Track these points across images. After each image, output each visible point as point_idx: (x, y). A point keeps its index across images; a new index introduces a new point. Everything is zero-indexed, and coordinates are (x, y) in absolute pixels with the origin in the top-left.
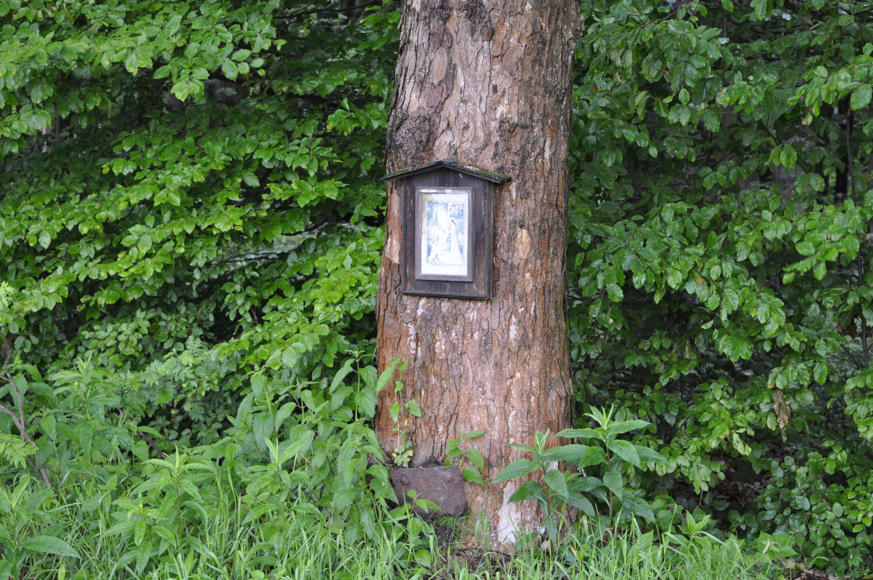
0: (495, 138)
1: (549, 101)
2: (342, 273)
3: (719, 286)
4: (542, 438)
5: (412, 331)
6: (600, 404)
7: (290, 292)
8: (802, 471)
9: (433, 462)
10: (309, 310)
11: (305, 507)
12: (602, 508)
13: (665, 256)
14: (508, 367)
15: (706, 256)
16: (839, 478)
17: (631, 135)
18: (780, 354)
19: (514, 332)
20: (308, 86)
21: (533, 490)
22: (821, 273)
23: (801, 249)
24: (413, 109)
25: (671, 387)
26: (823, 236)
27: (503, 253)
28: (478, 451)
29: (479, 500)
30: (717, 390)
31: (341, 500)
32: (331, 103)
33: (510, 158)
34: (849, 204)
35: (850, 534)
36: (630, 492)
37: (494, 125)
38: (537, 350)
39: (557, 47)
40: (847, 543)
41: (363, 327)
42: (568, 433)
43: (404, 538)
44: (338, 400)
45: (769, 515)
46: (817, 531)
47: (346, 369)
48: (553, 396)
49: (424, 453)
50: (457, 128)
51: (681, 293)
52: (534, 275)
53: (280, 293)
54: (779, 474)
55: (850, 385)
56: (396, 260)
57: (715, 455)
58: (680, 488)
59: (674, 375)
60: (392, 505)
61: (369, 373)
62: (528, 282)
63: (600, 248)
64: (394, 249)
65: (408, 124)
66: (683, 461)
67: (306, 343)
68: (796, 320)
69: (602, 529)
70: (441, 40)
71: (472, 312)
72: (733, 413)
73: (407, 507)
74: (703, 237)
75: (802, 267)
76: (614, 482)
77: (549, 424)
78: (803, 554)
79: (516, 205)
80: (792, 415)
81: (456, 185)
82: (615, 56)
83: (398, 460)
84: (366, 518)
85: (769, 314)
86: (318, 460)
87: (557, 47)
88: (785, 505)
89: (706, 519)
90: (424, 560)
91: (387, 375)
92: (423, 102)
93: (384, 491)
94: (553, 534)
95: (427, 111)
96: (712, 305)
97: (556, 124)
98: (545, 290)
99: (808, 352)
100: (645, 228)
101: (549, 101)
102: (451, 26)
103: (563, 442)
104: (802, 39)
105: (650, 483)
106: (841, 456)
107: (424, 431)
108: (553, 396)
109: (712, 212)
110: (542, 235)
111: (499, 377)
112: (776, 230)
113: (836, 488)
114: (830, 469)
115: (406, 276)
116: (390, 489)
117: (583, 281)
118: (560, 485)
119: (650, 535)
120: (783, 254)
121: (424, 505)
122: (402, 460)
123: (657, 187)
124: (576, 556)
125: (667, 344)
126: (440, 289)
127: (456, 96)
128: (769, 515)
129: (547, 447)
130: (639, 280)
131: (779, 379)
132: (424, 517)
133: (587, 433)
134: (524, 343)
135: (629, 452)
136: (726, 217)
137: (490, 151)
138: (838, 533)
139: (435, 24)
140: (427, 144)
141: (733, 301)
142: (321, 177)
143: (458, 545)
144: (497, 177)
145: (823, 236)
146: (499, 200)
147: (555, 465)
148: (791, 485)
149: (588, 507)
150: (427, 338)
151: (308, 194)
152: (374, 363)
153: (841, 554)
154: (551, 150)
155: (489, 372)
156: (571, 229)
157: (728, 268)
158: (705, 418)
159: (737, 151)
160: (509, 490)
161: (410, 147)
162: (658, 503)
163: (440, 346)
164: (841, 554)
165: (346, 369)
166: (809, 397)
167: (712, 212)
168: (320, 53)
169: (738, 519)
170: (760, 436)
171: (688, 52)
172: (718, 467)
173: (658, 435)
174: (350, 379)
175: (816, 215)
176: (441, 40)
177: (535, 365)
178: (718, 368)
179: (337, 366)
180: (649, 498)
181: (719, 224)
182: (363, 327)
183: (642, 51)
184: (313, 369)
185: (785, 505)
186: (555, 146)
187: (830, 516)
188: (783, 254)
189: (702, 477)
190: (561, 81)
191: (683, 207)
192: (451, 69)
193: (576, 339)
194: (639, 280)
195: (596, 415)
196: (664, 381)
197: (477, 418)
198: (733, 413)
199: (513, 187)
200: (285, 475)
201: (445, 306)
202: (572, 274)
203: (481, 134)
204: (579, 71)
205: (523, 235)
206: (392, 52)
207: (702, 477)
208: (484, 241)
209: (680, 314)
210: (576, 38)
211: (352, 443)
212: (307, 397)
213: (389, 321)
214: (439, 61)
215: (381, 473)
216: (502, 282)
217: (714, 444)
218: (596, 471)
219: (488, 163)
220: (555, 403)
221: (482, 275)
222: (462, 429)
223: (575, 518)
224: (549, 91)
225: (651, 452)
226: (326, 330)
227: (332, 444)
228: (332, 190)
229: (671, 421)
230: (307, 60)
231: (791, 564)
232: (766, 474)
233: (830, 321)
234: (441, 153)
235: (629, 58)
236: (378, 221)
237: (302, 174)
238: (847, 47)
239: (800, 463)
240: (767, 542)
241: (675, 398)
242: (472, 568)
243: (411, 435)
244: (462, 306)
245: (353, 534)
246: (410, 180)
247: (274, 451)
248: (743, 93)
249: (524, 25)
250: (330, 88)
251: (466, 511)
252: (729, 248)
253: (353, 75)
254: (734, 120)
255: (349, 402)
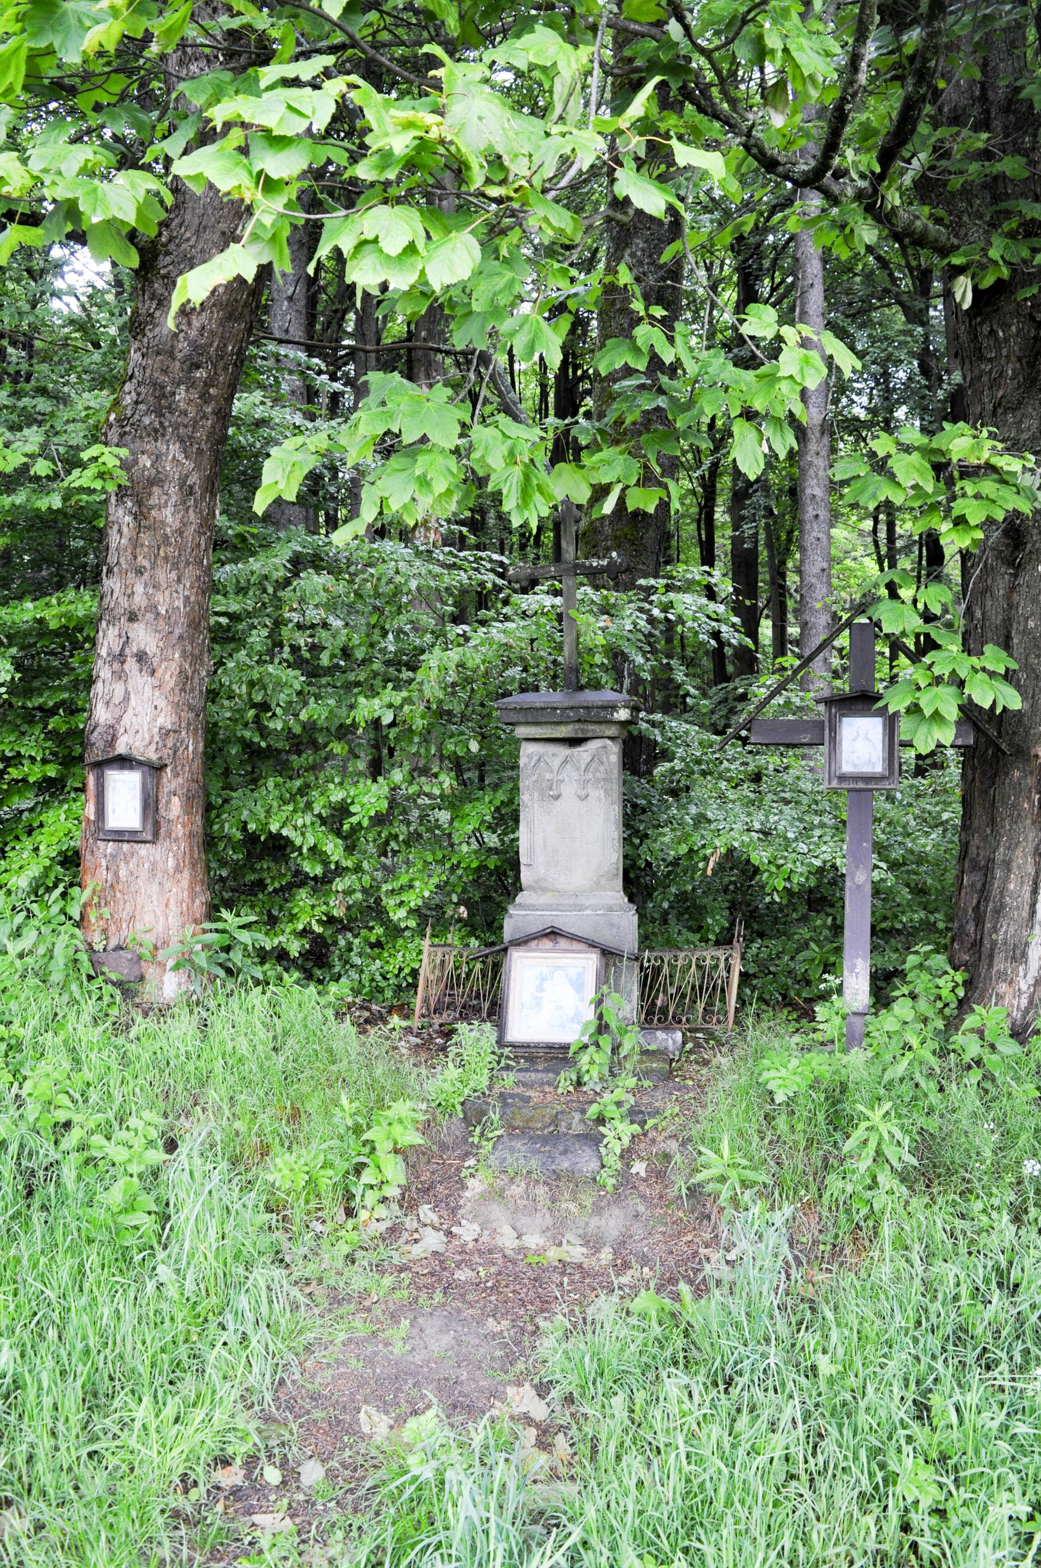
0: (157, 738)
1: (191, 715)
2: (57, 827)
3: (301, 830)
4: (190, 929)
5: (104, 863)
6: (229, 905)
7: (24, 838)
8: (357, 941)
9: (119, 948)
10: (36, 849)
11: (32, 981)
12: (229, 972)
13: (268, 812)
14: (168, 885)
15: (295, 811)
16: (378, 945)
17: (247, 734)
18: (340, 871)
19: (171, 863)
20: (38, 701)
21: (185, 963)
22: (365, 823)
23: (353, 809)
24: (102, 721)
25: (276, 891)
26: (365, 800)
27: (162, 812)
28: (149, 940)
29: (151, 972)
30: (303, 893)
31: (57, 977)
32: (52, 712)
33: (166, 751)
34: (380, 779)
35: (385, 978)
36: (249, 961)
37: (156, 730)
38: (186, 874)
39: (196, 680)
40: (383, 984)
41: (71, 860)
42: (208, 925)
43: (100, 999)
44: (55, 909)
45: (337, 969)
46: (366, 978)
47: (61, 889)
48: (198, 902)
49: (113, 943)
50: (131, 732)
51: (279, 836)
52: (184, 826)
53: (17, 838)
54: (342, 943)
55: (385, 887)
56: (92, 817)
57: (305, 932)
58: (281, 955)
59: (277, 885)
60: (90, 978)
61: (75, 891)
62: (179, 831)
63: (227, 806)
64: (90, 811)
65: (99, 730)
66: (282, 939)
67: (34, 870)
68: (350, 849)
69: (230, 985)
70: (120, 675)
71: (143, 850)
72: (313, 907)
73: (101, 978)
74: (293, 798)
75: (354, 820)
76: (236, 957)
77: (196, 922)
78: (356, 992)
79: (171, 782)
80: (349, 908)
81: (131, 768)
82: (235, 687)
83: (96, 948)
84: (74, 987)
85: (334, 848)
86: (42, 950)
87: (196, 680)
88: (347, 962)
89: (296, 975)
90: (114, 1011)
91: (88, 892)
92: (108, 715)
93: (86, 967)
94: (199, 990)
95: (111, 722)
96: (298, 842)
97: (196, 730)
98: (191, 835)
99: (358, 869)
100: (256, 795)
101: (191, 715)
102: (126, 667)
103: (204, 931)
104: (351, 677)
105: (263, 956)
106: (379, 930)
107: (113, 928)
108: (198, 902)
109: (298, 783)
110: (189, 800)
111: (161, 892)
112: (337, 795)
113: (377, 950)
114: (373, 939)
115: (98, 827)
116: (92, 966)
117: (216, 827)
118: (202, 959)
119: (260, 988)
120: (342, 810)
121: (114, 976)
122: (98, 947)
123: (264, 767)
124: (212, 1004)
125: (272, 864)
126: (120, 836)
127: (130, 712)
128: (337, 969)
129: (194, 935)
130: (252, 827)
131: (340, 884)
132: (114, 984)
133: (220, 925)
134: (178, 870)
135: (245, 937)
136: (307, 786)
137: (153, 747)
138: (379, 978)
139: (116, 666)
140: (112, 743)
141: (311, 841)
142: (44, 761)
143: (137, 1000)
144: (157, 765)
145: (365, 800)
146: (159, 778)
147: (199, 947)
148: (350, 950)
149: (222, 973)
150: (113, 868)
151: (35, 773)
152: (80, 885)
153: (381, 990)
154: (192, 746)
155: (155, 888)
156: (207, 795)
157: (308, 819)
158: (295, 911)
159: (316, 746)
160: (171, 963)
161: (100, 744)
162: (267, 966)
163: (123, 873)
164: (381, 990)
165: (61, 889)
166: (359, 896)
167: (298, 783)
168: (45, 679)
169: (318, 973)
170: (330, 920)
171: (280, 685)
172: (304, 941)
173: (265, 924)
174: (64, 895)
175: (361, 786)
176: (120, 675)
177: (185, 883)
178: (301, 879)
179: (55, 886)
180: (262, 963)
181: (302, 791)
182: (71, 860)
183: (252, 684)
184: (39, 889)
185: (347, 962)
186: (196, 743)
187: (373, 968)
188: (342, 810)
189: (294, 948)
190: (197, 702)
191: (280, 780)
192: (127, 694)
193: (213, 865)
194: (252, 827)
195: (225, 914)
196: (270, 889)
197: (148, 918)
198: (313, 907)
199: (168, 770)
200: (18, 963)
201: (126, 846)
202: (208, 823)
203: (147, 737)
204: (213, 695)
205: (176, 801)
206: (90, 681)
207: (294, 948)
208: (150, 805)
209: (278, 847)
210: (208, 675)
211: (62, 940)
212: (35, 908)
213: (88, 857)
214: (119, 689)
215: (83, 957)
216: (162, 831)
217: (300, 927)
218: (227, 949)
219: (153, 756)
220: (199, 906)
221: (149, 826)
222: (138, 925)
223: (212, 979)
224: (191, 708)
225: (260, 936)
226: (48, 863)
227: (50, 939)
228: (52, 771)
229: (275, 913)
230: (36, 684)
231: (350, 999)
232: (335, 943)
233: (372, 849)
234: (121, 749)
235: (244, 687)
236: (82, 790)
237: (33, 759)
238: (378, 682)
239: (356, 936)
240: (333, 988)
241: (277, 899)
242: (146, 1014)
243: (105, 931)
244: (136, 846)
245: (66, 998)
246: (100, 765)
247: (10, 947)
248: (314, 711)
249: (174, 667)
250: (51, 704)
251: (142, 978)
252: (309, 806)
253: (66, 695)
254: (310, 727)
255: (63, 912)
